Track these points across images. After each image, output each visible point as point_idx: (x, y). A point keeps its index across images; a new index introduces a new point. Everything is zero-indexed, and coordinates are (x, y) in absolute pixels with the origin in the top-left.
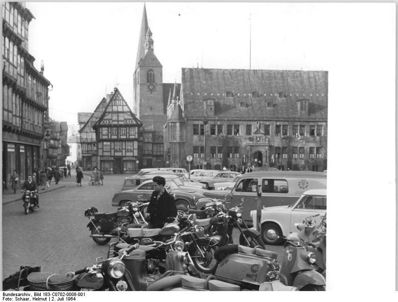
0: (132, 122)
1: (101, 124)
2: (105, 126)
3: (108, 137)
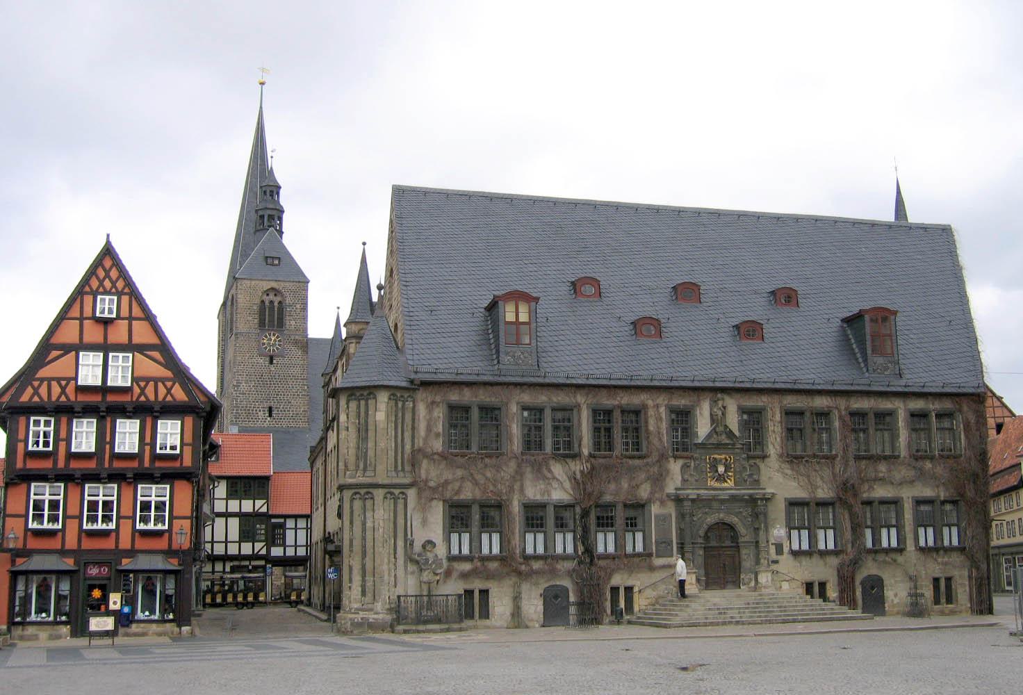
0: (169, 391)
2: (40, 410)
3: (55, 462)
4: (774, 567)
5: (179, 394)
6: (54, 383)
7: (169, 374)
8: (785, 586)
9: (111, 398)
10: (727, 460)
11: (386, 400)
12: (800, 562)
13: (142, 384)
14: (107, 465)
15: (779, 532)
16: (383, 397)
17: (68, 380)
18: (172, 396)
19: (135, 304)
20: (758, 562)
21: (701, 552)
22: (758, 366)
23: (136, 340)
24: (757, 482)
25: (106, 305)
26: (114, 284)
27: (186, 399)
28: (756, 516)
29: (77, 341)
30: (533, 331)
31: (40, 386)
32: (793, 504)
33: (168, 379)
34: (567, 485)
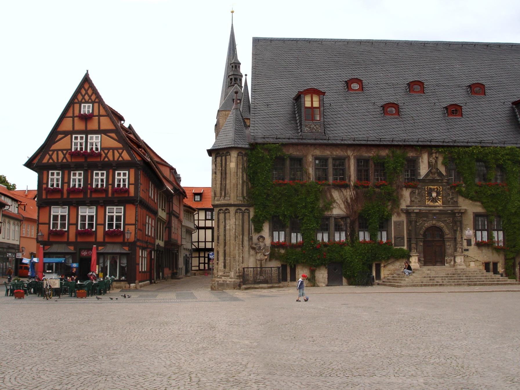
0: (120, 155)
1: (45, 161)
4: (466, 253)
5: (126, 156)
6: (60, 152)
7: (120, 145)
8: (472, 264)
9: (89, 160)
10: (438, 189)
11: (236, 156)
12: (482, 251)
13: (106, 151)
14: (89, 196)
15: (469, 232)
16: (234, 154)
17: (67, 150)
18: (122, 158)
19: (101, 108)
20: (455, 250)
21: (422, 244)
22: (458, 132)
23: (103, 127)
24: (456, 202)
25: (86, 109)
26: (90, 97)
27: (130, 159)
28: (455, 222)
29: (71, 129)
30: (322, 112)
31: (53, 154)
32: (477, 215)
33: (120, 148)
34: (343, 206)
